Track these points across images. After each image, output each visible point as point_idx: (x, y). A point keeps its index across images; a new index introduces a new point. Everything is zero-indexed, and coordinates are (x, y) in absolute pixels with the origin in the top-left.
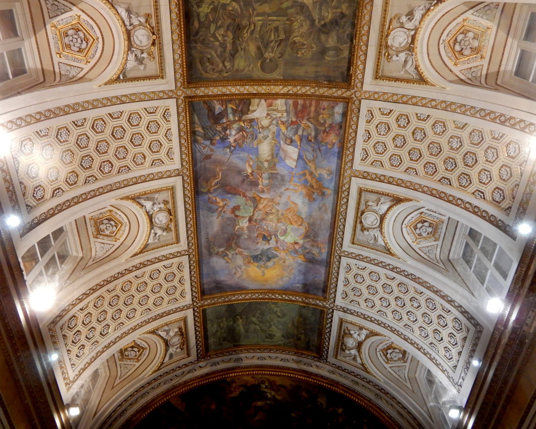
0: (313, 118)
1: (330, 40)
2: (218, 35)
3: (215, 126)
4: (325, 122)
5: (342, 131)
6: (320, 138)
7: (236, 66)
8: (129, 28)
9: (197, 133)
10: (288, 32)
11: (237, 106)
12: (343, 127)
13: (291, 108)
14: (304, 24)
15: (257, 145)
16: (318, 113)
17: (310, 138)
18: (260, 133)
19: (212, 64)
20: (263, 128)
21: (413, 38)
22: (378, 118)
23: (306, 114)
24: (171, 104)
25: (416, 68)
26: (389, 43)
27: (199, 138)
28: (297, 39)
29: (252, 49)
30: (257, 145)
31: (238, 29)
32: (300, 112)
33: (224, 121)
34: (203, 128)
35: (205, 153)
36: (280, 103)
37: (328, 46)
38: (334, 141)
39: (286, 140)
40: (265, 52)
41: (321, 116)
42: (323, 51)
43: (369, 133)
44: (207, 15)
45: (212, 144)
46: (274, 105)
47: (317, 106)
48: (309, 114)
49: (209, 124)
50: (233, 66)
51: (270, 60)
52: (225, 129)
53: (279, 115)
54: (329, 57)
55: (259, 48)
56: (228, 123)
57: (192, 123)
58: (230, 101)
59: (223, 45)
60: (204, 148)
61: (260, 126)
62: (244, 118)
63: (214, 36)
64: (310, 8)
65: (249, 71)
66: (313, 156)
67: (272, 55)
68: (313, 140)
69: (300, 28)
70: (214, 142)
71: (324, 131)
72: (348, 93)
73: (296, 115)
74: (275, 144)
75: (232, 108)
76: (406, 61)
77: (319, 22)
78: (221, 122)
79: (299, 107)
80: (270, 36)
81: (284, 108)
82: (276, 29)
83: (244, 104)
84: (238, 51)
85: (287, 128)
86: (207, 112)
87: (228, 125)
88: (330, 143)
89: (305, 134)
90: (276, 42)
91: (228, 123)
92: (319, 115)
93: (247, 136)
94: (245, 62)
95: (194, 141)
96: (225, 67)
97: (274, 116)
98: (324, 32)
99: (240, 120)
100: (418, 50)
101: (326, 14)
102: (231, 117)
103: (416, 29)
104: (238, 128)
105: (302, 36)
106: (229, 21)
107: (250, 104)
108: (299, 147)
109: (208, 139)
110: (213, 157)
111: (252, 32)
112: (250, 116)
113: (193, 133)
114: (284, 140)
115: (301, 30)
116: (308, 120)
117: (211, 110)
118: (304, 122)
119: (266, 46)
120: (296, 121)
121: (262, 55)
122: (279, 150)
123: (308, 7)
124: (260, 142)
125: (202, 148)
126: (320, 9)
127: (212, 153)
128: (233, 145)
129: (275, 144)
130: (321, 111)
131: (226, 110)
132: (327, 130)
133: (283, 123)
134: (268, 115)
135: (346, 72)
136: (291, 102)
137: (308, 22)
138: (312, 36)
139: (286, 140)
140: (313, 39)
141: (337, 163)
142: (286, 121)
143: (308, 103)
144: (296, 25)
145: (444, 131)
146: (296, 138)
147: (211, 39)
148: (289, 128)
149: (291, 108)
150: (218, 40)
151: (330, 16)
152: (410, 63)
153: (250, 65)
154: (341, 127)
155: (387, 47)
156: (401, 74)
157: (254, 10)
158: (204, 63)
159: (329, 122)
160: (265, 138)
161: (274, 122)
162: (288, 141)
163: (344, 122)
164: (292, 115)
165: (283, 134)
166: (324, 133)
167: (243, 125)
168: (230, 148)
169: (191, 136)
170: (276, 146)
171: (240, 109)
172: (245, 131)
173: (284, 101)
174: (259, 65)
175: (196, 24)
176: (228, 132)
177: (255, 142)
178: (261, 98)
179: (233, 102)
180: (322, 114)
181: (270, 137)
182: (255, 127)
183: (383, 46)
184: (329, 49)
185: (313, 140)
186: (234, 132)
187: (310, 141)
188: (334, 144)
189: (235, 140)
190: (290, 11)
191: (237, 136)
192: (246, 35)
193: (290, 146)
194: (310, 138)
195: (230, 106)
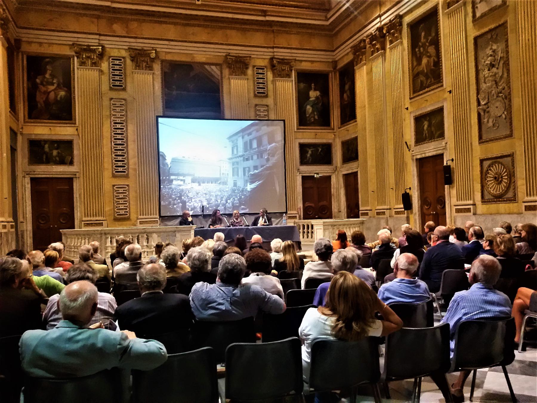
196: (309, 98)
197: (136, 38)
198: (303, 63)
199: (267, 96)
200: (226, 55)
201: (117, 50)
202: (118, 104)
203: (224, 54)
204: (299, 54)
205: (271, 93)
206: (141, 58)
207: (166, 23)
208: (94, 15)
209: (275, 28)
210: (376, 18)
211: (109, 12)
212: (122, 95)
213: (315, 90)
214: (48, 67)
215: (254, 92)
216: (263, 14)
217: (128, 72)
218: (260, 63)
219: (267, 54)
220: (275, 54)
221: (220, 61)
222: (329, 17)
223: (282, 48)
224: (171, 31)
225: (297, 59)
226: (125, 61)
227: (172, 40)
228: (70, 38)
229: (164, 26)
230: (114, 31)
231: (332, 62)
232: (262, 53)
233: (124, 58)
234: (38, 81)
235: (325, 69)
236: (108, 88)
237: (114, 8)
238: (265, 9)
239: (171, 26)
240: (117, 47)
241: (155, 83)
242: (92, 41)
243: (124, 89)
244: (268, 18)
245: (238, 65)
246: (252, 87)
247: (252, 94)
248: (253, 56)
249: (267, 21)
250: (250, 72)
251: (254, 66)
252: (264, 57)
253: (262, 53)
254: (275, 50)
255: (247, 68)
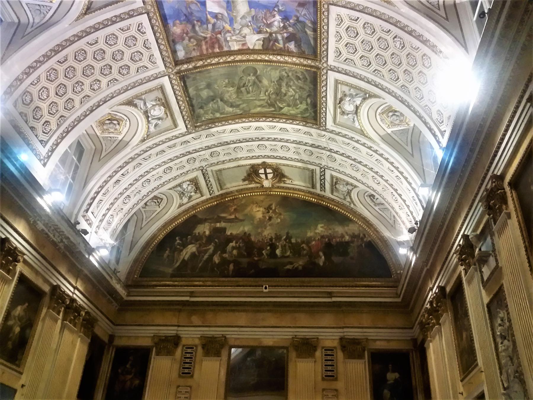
0: (202, 41)
1: (206, 93)
2: (293, 92)
3: (294, 32)
4: (189, 40)
5: (171, 39)
6: (189, 27)
7: (278, 72)
8: (355, 116)
9: (311, 29)
10: (239, 91)
11: (274, 45)
12: (171, 43)
13: (224, 44)
14: (228, 98)
15: (250, 11)
16: (199, 45)
17: (199, 23)
18: (250, 22)
19: (297, 76)
20: (248, 26)
21: (148, 117)
22: (145, 61)
23: (209, 42)
24: (332, 61)
25: (136, 106)
26: (162, 108)
27: (310, 25)
28: (231, 89)
29: (265, 82)
30: (250, 11)
31: (278, 93)
32: (214, 42)
33: (285, 35)
34: (306, 32)
35: (304, 10)
36: (235, 47)
37: (206, 90)
38: (175, 28)
39: (222, 17)
40: (254, 80)
41: (194, 44)
42: (209, 86)
43: (147, 48)
44: (301, 103)
45: (298, 18)
46: (241, 45)
47: (201, 51)
48: (206, 42)
49: (299, 35)
50: (280, 72)
51: (250, 75)
52: (285, 27)
53: (234, 38)
54: (203, 85)
55: (260, 82)
56: (281, 32)
57: (315, 39)
58: (281, 49)
59: (288, 86)
60: (305, 15)
61: (251, 28)
62: (267, 35)
63: (296, 92)
64: (226, 106)
65: (267, 68)
66: (190, 8)
67: (249, 78)
68: (195, 22)
69: (230, 93)
70: (295, 19)
71: (187, 34)
72: (178, 68)
73: (218, 40)
74: (233, 13)
75: (279, 44)
76: (145, 104)
77: (218, 101)
78: (289, 34)
79: (217, 46)
80: (253, 89)
81: (230, 43)
82: (248, 92)
83: (269, 46)
84: (277, 81)
85: (224, 28)
86: (302, 45)
87: (283, 30)
88: (177, 25)
89: (205, 26)
90: (247, 86)
91: (281, 32)
92: (196, 45)
93: (262, 19)
94: (270, 74)
95: (315, 23)
96: (286, 73)
97: (239, 36)
98: (212, 96)
99: (271, 34)
100: (141, 114)
101: (214, 105)
102: (280, 37)
103: (149, 122)
104: (272, 27)
105: (228, 91)
106: (285, 98)
107: (263, 45)
108: (207, 13)
109: (300, 22)
110: (297, 4)
111: (267, 91)
112: (261, 36)
113: (315, 30)
114: (224, 17)
115: (229, 94)
116: (205, 38)
117: (298, 45)
118: (209, 35)
119: (254, 83)
120: (216, 35)
121: (257, 77)
122: (228, 7)
123: (228, 106)
124: (248, 13)
125: (308, 16)
126: (218, 107)
127: (298, 8)
128: (276, 13)
129: (233, 13)
130: (196, 48)
131: (284, 44)
132: (185, 35)
133: (229, 31)
134: (244, 37)
135: (186, 79)
136: (226, 49)
137: (225, 99)
138: (220, 92)
139: (222, 17)
140: (219, 91)
141: (163, 9)
142: (226, 33)
143: (210, 51)
144: (234, 96)
145: (91, 86)
146: (213, 21)
147: (298, 91)
148: (222, 28)
149: (224, 44)
150: (293, 89)
151: (211, 105)
152: (142, 106)
153: (266, 72)
154: (173, 41)
155: (163, 105)
156: (143, 97)
157: (267, 102)
158: (303, 78)
159: (186, 41)
160: (243, 17)
161: (238, 32)
162: (220, 16)
163: (172, 47)
164: (222, 39)
165: (226, 23)
166: (187, 31)
167: (267, 29)
168: (279, 9)
169: (317, 27)
170: (230, 10)
171: (272, 42)
172: (265, 24)
173: (232, 49)
174: (259, 72)
175: (309, 101)
176: (282, 25)
177: (253, 12)
178: (252, 50)
179: (278, 48)
180: (194, 46)
181: (239, 19)
182: (255, 26)
183: (166, 105)
184: (205, 88)
185: (195, 22)
186: (276, 23)
187: (198, 21)
188: (174, 25)
189: (274, 16)
190: (240, 103)
191: (273, 20)
192: (271, 90)
193: (217, 12)
194: (199, 23)
195: (281, 46)
196: (387, 381)
197: (209, 326)
198: (378, 343)
199: (336, 379)
200: (293, 338)
201: (191, 339)
202: (184, 391)
203: (291, 337)
204: (372, 333)
205: (341, 377)
206: (213, 346)
207: (238, 311)
208: (176, 309)
209: (344, 308)
210: (429, 292)
211: (189, 305)
212: (190, 382)
213: (393, 371)
214: (131, 358)
215: (322, 374)
216: (329, 296)
217: (198, 358)
218: (328, 344)
219: (337, 334)
220: (345, 334)
221: (286, 344)
222: (399, 292)
223: (352, 327)
224: (242, 318)
225: (369, 338)
226: (196, 350)
227: (242, 327)
228: (151, 331)
229: (237, 314)
230: (192, 323)
231: (411, 339)
232: (331, 334)
233: (196, 346)
234: (120, 371)
235: (403, 348)
236: (177, 376)
237: (193, 302)
238: (330, 291)
239: (243, 314)
240: (191, 334)
241: (221, 369)
242: (171, 331)
243: (192, 376)
244: (334, 299)
245: (306, 347)
246: (320, 370)
247: (320, 378)
248: (320, 337)
249: (334, 302)
250: (318, 353)
251: (323, 348)
252: (334, 338)
253: (331, 334)
254: (345, 330)
255: (315, 350)
